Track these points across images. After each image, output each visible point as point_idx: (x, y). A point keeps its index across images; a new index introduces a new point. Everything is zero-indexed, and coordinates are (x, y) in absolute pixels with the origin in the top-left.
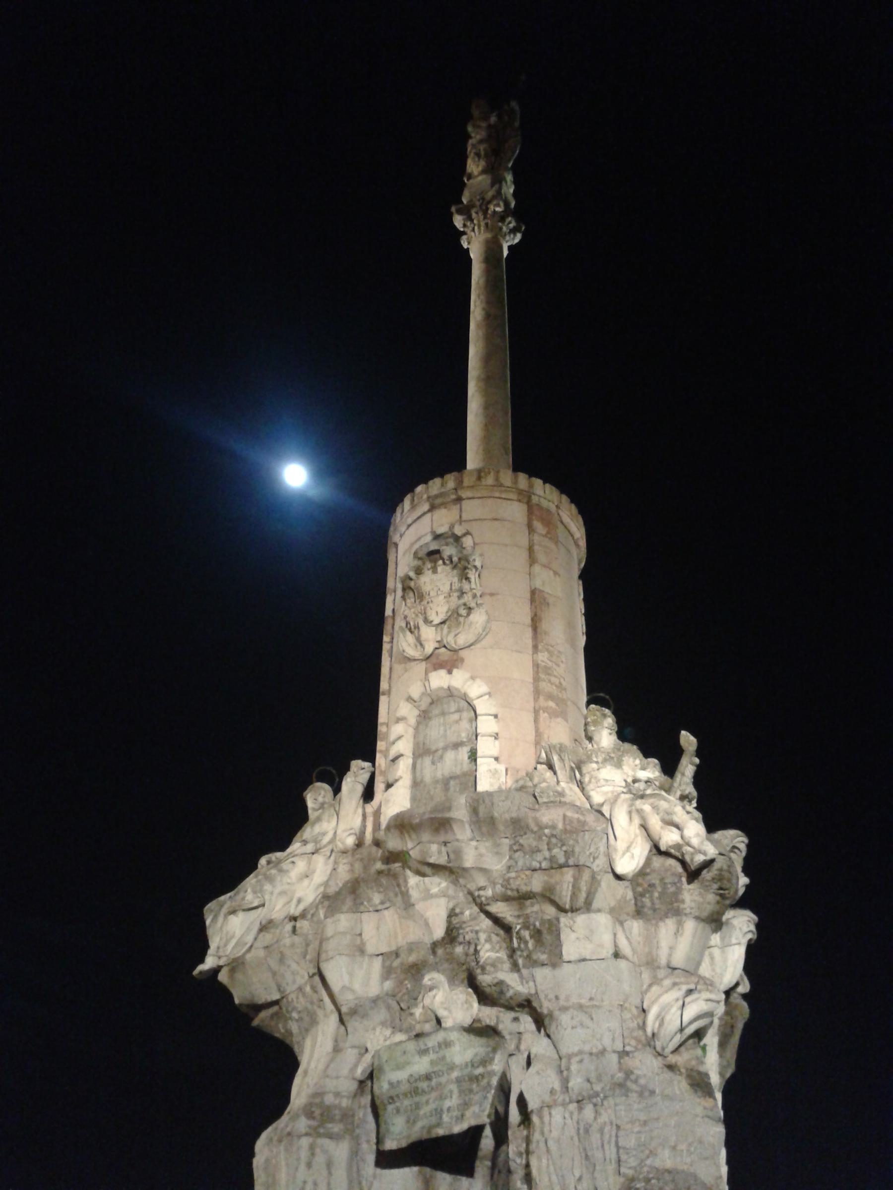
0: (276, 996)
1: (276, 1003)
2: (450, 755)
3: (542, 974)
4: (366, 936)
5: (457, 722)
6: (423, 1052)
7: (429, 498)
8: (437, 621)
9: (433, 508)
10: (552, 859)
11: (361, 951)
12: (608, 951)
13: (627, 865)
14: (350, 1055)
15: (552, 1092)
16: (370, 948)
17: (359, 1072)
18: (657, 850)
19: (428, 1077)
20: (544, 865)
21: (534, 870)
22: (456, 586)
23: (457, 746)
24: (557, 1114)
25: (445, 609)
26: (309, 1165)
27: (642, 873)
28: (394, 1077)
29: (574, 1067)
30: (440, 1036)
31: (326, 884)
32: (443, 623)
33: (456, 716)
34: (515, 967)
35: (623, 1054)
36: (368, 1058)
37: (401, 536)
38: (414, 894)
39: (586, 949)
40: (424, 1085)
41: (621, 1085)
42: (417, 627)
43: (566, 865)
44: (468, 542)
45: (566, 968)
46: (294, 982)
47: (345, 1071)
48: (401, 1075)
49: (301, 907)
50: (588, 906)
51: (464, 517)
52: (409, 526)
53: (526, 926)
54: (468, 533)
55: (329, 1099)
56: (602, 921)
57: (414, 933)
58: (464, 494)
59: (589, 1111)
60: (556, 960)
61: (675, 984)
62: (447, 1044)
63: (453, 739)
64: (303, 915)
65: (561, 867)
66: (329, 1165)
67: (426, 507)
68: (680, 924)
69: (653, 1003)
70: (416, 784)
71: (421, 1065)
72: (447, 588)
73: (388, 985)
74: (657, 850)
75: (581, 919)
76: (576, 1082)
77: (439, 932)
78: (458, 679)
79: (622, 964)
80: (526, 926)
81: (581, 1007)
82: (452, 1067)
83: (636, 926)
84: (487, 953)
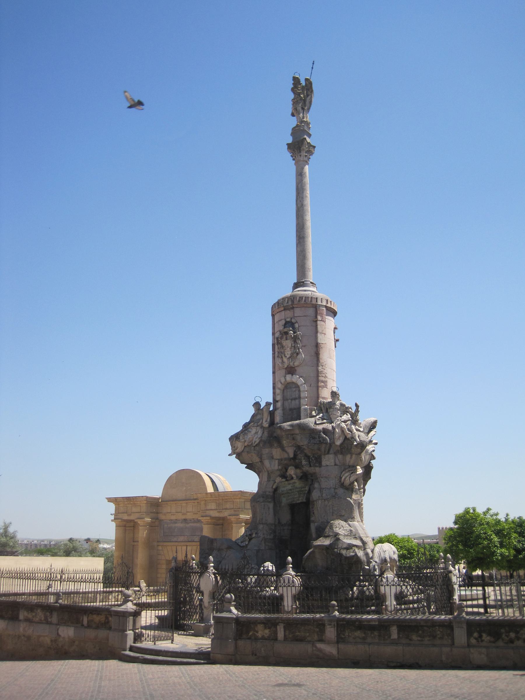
0: (251, 463)
2: (293, 402)
3: (317, 469)
4: (273, 454)
5: (295, 391)
6: (289, 484)
7: (283, 306)
8: (288, 357)
9: (284, 310)
10: (320, 441)
11: (272, 458)
12: (333, 464)
13: (338, 443)
14: (272, 482)
15: (319, 497)
16: (275, 457)
17: (274, 487)
19: (291, 490)
20: (318, 442)
21: (315, 444)
22: (293, 345)
23: (295, 399)
24: (320, 502)
25: (290, 353)
26: (264, 509)
27: (342, 444)
28: (282, 489)
29: (324, 491)
30: (293, 481)
31: (261, 437)
32: (290, 357)
33: (294, 389)
34: (310, 466)
35: (335, 489)
36: (276, 484)
38: (285, 445)
39: (328, 463)
40: (290, 491)
41: (334, 496)
42: (282, 357)
43: (323, 443)
44: (296, 325)
45: (323, 468)
47: (271, 487)
48: (285, 489)
49: (256, 443)
50: (328, 453)
51: (295, 315)
53: (313, 457)
54: (297, 322)
55: (267, 493)
56: (331, 456)
57: (286, 456)
58: (295, 306)
59: (326, 502)
60: (320, 465)
61: (349, 471)
62: (295, 483)
63: (294, 397)
64: (256, 445)
65: (322, 443)
66: (269, 508)
67: (283, 309)
68: (351, 456)
69: (343, 475)
70: (284, 409)
71: (289, 487)
72: (290, 345)
73: (280, 467)
74: (346, 438)
75: (327, 456)
76: (324, 495)
77: (292, 456)
78: (295, 378)
79: (336, 467)
80: (313, 457)
81: (326, 477)
82: (297, 488)
83: (340, 457)
84: (304, 462)
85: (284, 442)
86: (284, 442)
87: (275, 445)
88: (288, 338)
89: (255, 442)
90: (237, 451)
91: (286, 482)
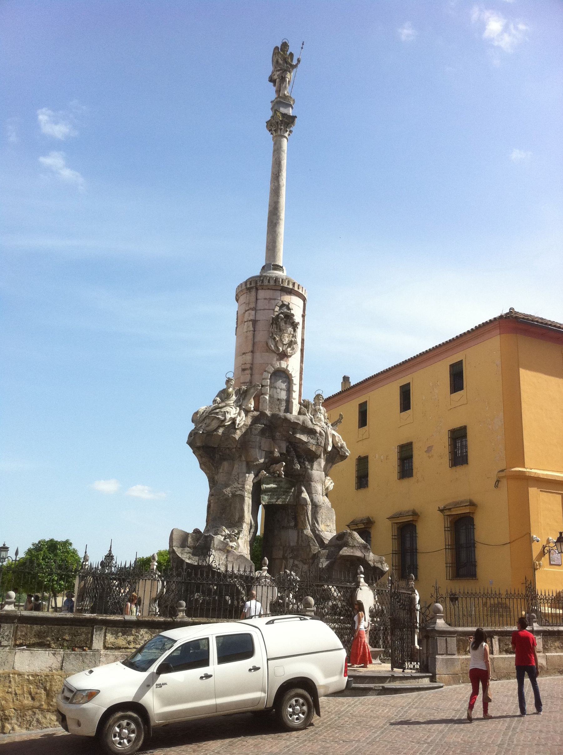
1: (214, 448)
8: (285, 343)
10: (318, 443)
16: (262, 448)
17: (255, 481)
18: (334, 446)
30: (280, 479)
36: (258, 478)
37: (262, 289)
38: (277, 437)
46: (227, 445)
49: (240, 426)
52: (268, 289)
60: (312, 468)
62: (281, 481)
82: (281, 487)
85: (278, 434)
86: (278, 434)
87: (267, 435)
88: (288, 322)
89: (239, 424)
90: (208, 429)
91: (272, 479)
